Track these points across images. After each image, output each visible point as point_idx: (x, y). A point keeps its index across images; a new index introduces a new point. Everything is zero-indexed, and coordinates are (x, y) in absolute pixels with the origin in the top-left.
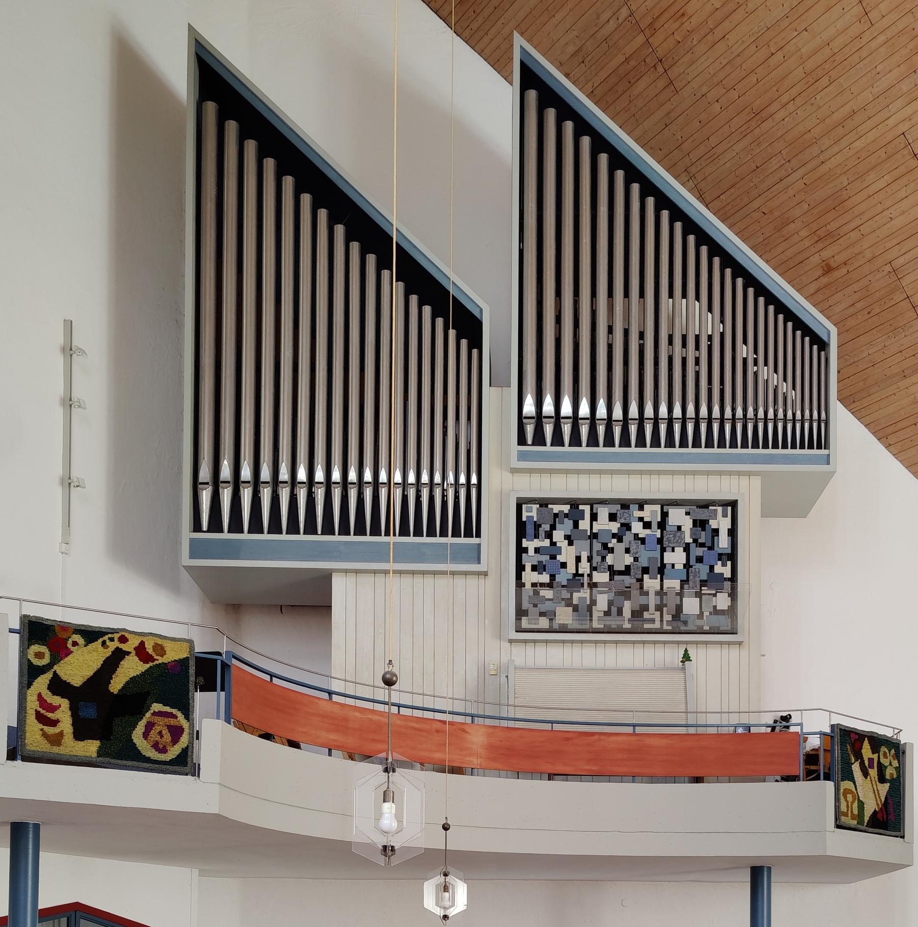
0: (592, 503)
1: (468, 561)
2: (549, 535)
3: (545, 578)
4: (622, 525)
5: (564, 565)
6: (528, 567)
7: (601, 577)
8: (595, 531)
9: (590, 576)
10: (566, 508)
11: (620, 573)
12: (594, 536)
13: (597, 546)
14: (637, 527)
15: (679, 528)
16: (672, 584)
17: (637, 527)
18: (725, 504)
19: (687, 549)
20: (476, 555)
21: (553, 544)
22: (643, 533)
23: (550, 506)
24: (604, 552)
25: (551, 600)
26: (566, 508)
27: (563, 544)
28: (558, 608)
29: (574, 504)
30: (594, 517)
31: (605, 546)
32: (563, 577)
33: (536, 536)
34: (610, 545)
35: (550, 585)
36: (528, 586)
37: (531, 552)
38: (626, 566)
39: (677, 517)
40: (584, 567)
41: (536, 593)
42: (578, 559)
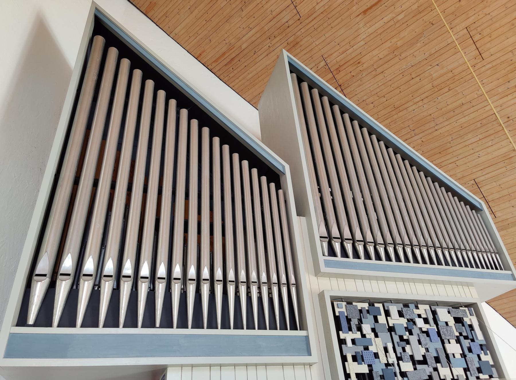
0: (383, 301)
1: (299, 353)
2: (360, 329)
5: (376, 355)
7: (407, 366)
8: (391, 325)
9: (399, 365)
10: (366, 306)
11: (420, 362)
12: (391, 329)
13: (396, 339)
14: (420, 323)
15: (447, 323)
17: (420, 323)
18: (468, 306)
19: (458, 341)
21: (363, 336)
22: (425, 327)
24: (403, 343)
27: (370, 335)
30: (387, 314)
31: (401, 338)
33: (350, 329)
34: (405, 337)
37: (349, 343)
38: (423, 356)
39: (443, 315)
40: (392, 359)
42: (386, 350)
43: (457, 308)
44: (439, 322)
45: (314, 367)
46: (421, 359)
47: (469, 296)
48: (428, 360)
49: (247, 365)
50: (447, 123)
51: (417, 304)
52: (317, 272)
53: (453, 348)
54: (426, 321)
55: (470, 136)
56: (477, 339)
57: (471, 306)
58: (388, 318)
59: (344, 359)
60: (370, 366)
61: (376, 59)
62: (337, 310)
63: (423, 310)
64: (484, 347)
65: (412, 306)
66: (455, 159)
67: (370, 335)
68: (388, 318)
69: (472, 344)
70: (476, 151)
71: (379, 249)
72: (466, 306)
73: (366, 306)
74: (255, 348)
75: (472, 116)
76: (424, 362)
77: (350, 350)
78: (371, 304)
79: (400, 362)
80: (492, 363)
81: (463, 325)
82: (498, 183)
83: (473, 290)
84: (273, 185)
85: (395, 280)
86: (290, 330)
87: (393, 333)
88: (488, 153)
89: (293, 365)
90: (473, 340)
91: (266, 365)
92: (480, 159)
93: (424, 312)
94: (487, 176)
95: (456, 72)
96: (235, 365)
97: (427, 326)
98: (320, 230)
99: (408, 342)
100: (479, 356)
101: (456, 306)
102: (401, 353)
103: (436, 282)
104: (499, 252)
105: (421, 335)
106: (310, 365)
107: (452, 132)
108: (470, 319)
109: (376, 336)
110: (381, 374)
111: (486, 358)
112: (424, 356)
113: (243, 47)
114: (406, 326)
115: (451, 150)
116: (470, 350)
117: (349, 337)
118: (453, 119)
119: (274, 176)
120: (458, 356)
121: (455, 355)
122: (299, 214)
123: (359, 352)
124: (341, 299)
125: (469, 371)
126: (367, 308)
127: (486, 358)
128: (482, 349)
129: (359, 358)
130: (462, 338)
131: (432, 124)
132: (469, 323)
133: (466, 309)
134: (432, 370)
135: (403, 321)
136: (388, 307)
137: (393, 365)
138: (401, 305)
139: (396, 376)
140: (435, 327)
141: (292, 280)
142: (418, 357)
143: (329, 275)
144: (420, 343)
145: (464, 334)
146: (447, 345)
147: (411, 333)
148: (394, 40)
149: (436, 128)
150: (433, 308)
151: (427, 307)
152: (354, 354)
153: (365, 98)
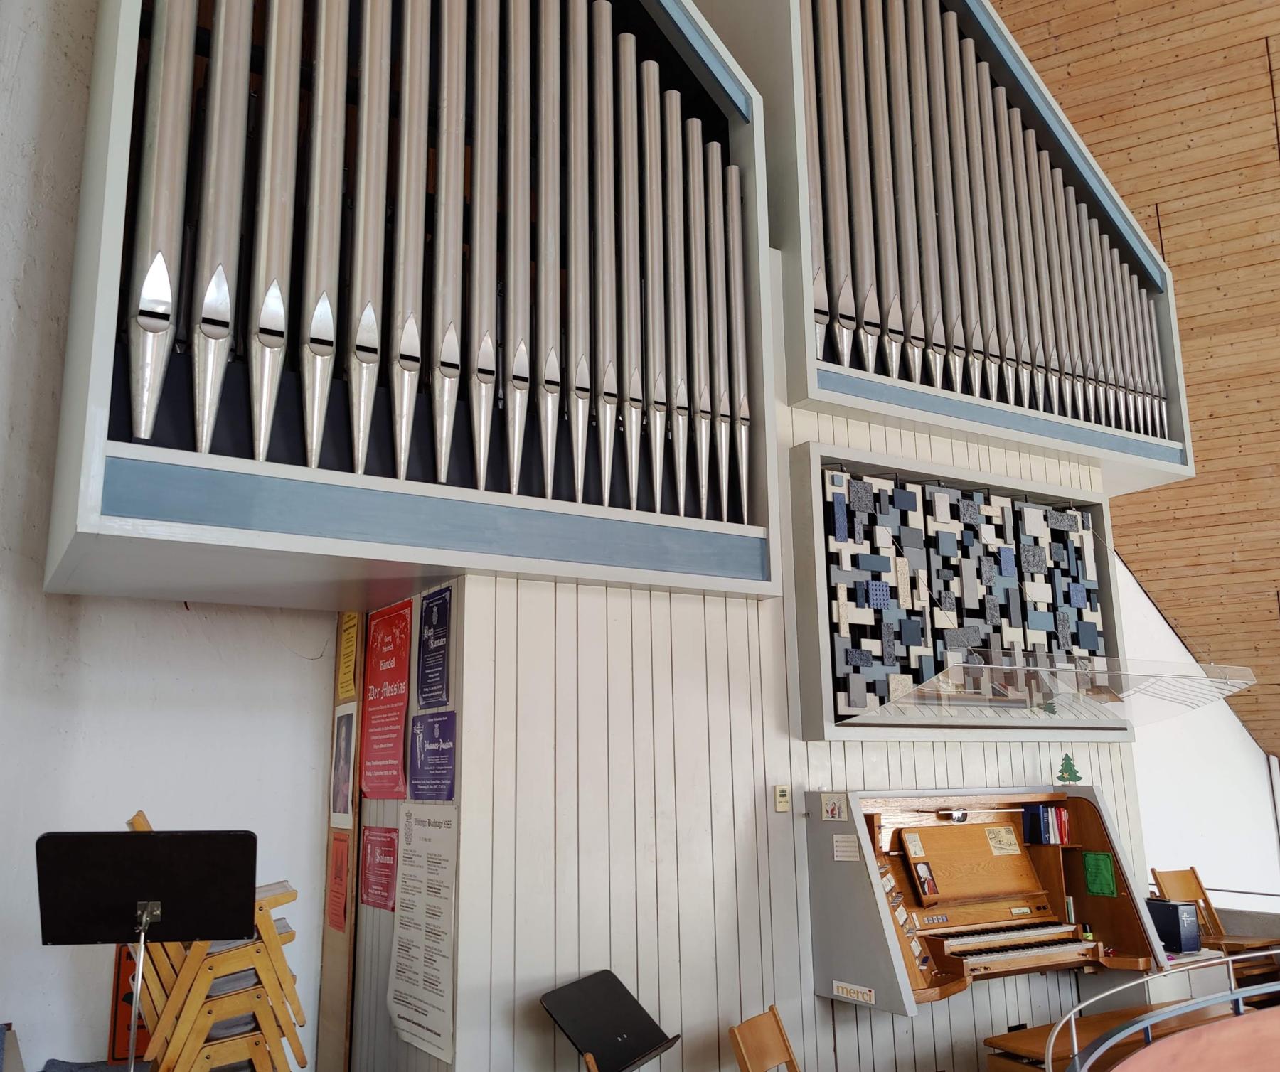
0: (924, 480)
1: (742, 572)
2: (869, 535)
3: (865, 617)
4: (968, 527)
5: (894, 592)
6: (842, 594)
7: (945, 619)
8: (931, 533)
11: (973, 614)
12: (931, 542)
13: (937, 563)
14: (988, 533)
15: (1036, 540)
16: (1038, 637)
17: (988, 533)
18: (1083, 507)
19: (1049, 579)
20: (758, 561)
21: (875, 550)
22: (994, 543)
23: (866, 479)
24: (948, 573)
25: (880, 659)
26: (888, 486)
27: (887, 550)
28: (891, 677)
29: (901, 479)
30: (929, 509)
31: (946, 561)
32: (893, 617)
33: (851, 534)
34: (954, 562)
35: (875, 631)
36: (845, 631)
37: (846, 563)
39: (1036, 523)
40: (923, 602)
41: (856, 645)
42: (913, 583)
43: (1063, 510)
44: (1022, 537)
45: (766, 606)
46: (976, 606)
47: (1086, 487)
48: (988, 611)
49: (631, 587)
51: (989, 493)
52: (796, 394)
53: (1039, 592)
54: (1000, 532)
56: (1085, 577)
57: (1089, 509)
58: (929, 517)
59: (832, 593)
60: (878, 612)
62: (830, 489)
63: (999, 507)
64: (1093, 596)
65: (978, 497)
66: (1133, 141)
67: (887, 550)
68: (929, 517)
69: (1073, 586)
70: (1188, 130)
71: (931, 357)
72: (1078, 509)
73: (888, 486)
74: (655, 553)
75: (1212, 30)
76: (980, 613)
78: (900, 485)
79: (936, 609)
80: (1100, 627)
81: (1066, 548)
82: (1208, 225)
83: (1096, 474)
84: (715, 147)
85: (952, 434)
86: (729, 521)
87: (932, 551)
88: (1213, 142)
89: (726, 595)
90: (1076, 580)
91: (670, 590)
92: (1189, 153)
93: (999, 513)
94: (1188, 202)
96: (607, 585)
97: (1000, 542)
98: (813, 293)
99: (957, 571)
101: (1061, 505)
102: (940, 592)
103: (1030, 449)
104: (1169, 397)
105: (984, 559)
106: (759, 599)
107: (1152, 65)
108: (1081, 537)
109: (899, 554)
110: (897, 629)
111: (1093, 617)
112: (982, 602)
114: (959, 538)
115: (1130, 114)
116: (1067, 598)
117: (847, 549)
118: (1165, 29)
120: (1043, 608)
121: (1039, 605)
122: (775, 243)
123: (861, 583)
124: (839, 465)
125: (1057, 638)
126: (890, 493)
127: (1093, 617)
128: (1089, 599)
129: (860, 594)
130: (1057, 573)
131: (1110, 30)
132: (1077, 544)
133: (1078, 514)
134: (989, 629)
135: (956, 528)
136: (932, 494)
137: (920, 614)
138: (958, 494)
139: (923, 634)
140: (1013, 547)
141: (744, 411)
142: (971, 603)
143: (821, 407)
144: (979, 576)
145: (1064, 565)
146: (1028, 585)
147: (966, 554)
149: (1115, 44)
150: (1018, 505)
152: (852, 586)
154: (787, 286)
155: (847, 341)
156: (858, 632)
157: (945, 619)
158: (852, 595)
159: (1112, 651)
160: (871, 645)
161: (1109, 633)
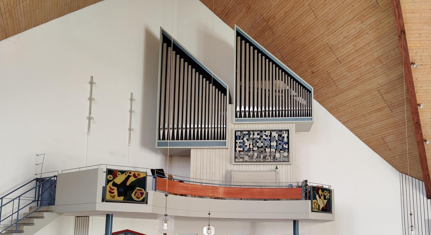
2: (243, 139)
3: (242, 149)
6: (238, 147)
7: (255, 149)
10: (247, 132)
11: (260, 148)
12: (253, 139)
16: (274, 150)
18: (286, 131)
19: (277, 141)
26: (247, 132)
27: (246, 141)
29: (249, 131)
30: (254, 134)
31: (256, 141)
32: (246, 149)
35: (243, 151)
36: (238, 151)
37: (238, 143)
39: (274, 134)
40: (251, 146)
42: (250, 144)
50: (312, 47)
55: (321, 52)
61: (280, 16)
63: (268, 133)
77: (238, 145)
82: (336, 73)
95: (310, 24)
100: (283, 146)
113: (230, 8)
119: (223, 90)
124: (238, 131)
148: (285, 8)
151: (269, 132)
153: (281, 34)
154: (231, 109)
155: (239, 115)
156: (240, 151)
157: (255, 149)
158: (239, 147)
159: (288, 152)
160: (242, 153)
161: (288, 149)
